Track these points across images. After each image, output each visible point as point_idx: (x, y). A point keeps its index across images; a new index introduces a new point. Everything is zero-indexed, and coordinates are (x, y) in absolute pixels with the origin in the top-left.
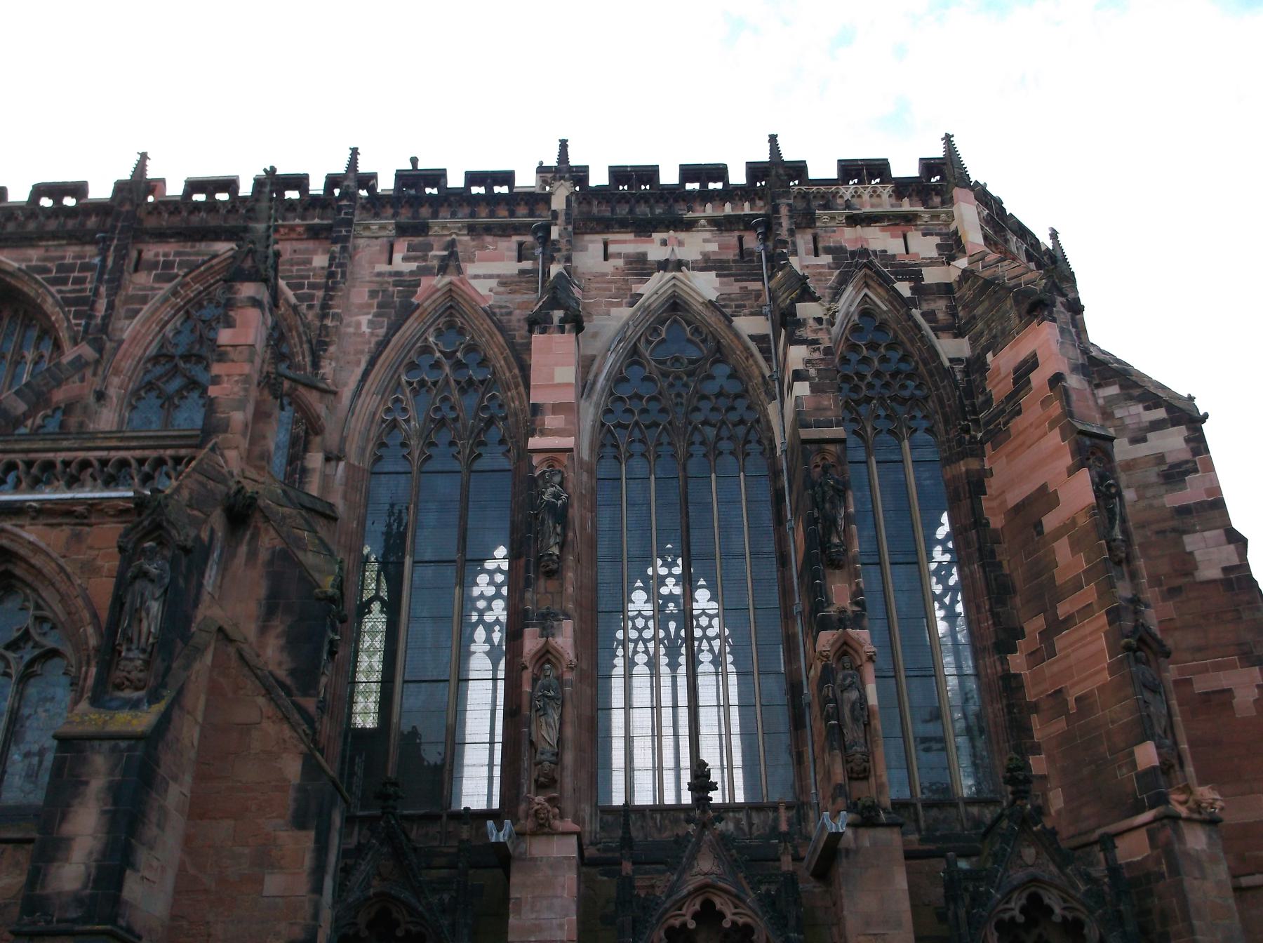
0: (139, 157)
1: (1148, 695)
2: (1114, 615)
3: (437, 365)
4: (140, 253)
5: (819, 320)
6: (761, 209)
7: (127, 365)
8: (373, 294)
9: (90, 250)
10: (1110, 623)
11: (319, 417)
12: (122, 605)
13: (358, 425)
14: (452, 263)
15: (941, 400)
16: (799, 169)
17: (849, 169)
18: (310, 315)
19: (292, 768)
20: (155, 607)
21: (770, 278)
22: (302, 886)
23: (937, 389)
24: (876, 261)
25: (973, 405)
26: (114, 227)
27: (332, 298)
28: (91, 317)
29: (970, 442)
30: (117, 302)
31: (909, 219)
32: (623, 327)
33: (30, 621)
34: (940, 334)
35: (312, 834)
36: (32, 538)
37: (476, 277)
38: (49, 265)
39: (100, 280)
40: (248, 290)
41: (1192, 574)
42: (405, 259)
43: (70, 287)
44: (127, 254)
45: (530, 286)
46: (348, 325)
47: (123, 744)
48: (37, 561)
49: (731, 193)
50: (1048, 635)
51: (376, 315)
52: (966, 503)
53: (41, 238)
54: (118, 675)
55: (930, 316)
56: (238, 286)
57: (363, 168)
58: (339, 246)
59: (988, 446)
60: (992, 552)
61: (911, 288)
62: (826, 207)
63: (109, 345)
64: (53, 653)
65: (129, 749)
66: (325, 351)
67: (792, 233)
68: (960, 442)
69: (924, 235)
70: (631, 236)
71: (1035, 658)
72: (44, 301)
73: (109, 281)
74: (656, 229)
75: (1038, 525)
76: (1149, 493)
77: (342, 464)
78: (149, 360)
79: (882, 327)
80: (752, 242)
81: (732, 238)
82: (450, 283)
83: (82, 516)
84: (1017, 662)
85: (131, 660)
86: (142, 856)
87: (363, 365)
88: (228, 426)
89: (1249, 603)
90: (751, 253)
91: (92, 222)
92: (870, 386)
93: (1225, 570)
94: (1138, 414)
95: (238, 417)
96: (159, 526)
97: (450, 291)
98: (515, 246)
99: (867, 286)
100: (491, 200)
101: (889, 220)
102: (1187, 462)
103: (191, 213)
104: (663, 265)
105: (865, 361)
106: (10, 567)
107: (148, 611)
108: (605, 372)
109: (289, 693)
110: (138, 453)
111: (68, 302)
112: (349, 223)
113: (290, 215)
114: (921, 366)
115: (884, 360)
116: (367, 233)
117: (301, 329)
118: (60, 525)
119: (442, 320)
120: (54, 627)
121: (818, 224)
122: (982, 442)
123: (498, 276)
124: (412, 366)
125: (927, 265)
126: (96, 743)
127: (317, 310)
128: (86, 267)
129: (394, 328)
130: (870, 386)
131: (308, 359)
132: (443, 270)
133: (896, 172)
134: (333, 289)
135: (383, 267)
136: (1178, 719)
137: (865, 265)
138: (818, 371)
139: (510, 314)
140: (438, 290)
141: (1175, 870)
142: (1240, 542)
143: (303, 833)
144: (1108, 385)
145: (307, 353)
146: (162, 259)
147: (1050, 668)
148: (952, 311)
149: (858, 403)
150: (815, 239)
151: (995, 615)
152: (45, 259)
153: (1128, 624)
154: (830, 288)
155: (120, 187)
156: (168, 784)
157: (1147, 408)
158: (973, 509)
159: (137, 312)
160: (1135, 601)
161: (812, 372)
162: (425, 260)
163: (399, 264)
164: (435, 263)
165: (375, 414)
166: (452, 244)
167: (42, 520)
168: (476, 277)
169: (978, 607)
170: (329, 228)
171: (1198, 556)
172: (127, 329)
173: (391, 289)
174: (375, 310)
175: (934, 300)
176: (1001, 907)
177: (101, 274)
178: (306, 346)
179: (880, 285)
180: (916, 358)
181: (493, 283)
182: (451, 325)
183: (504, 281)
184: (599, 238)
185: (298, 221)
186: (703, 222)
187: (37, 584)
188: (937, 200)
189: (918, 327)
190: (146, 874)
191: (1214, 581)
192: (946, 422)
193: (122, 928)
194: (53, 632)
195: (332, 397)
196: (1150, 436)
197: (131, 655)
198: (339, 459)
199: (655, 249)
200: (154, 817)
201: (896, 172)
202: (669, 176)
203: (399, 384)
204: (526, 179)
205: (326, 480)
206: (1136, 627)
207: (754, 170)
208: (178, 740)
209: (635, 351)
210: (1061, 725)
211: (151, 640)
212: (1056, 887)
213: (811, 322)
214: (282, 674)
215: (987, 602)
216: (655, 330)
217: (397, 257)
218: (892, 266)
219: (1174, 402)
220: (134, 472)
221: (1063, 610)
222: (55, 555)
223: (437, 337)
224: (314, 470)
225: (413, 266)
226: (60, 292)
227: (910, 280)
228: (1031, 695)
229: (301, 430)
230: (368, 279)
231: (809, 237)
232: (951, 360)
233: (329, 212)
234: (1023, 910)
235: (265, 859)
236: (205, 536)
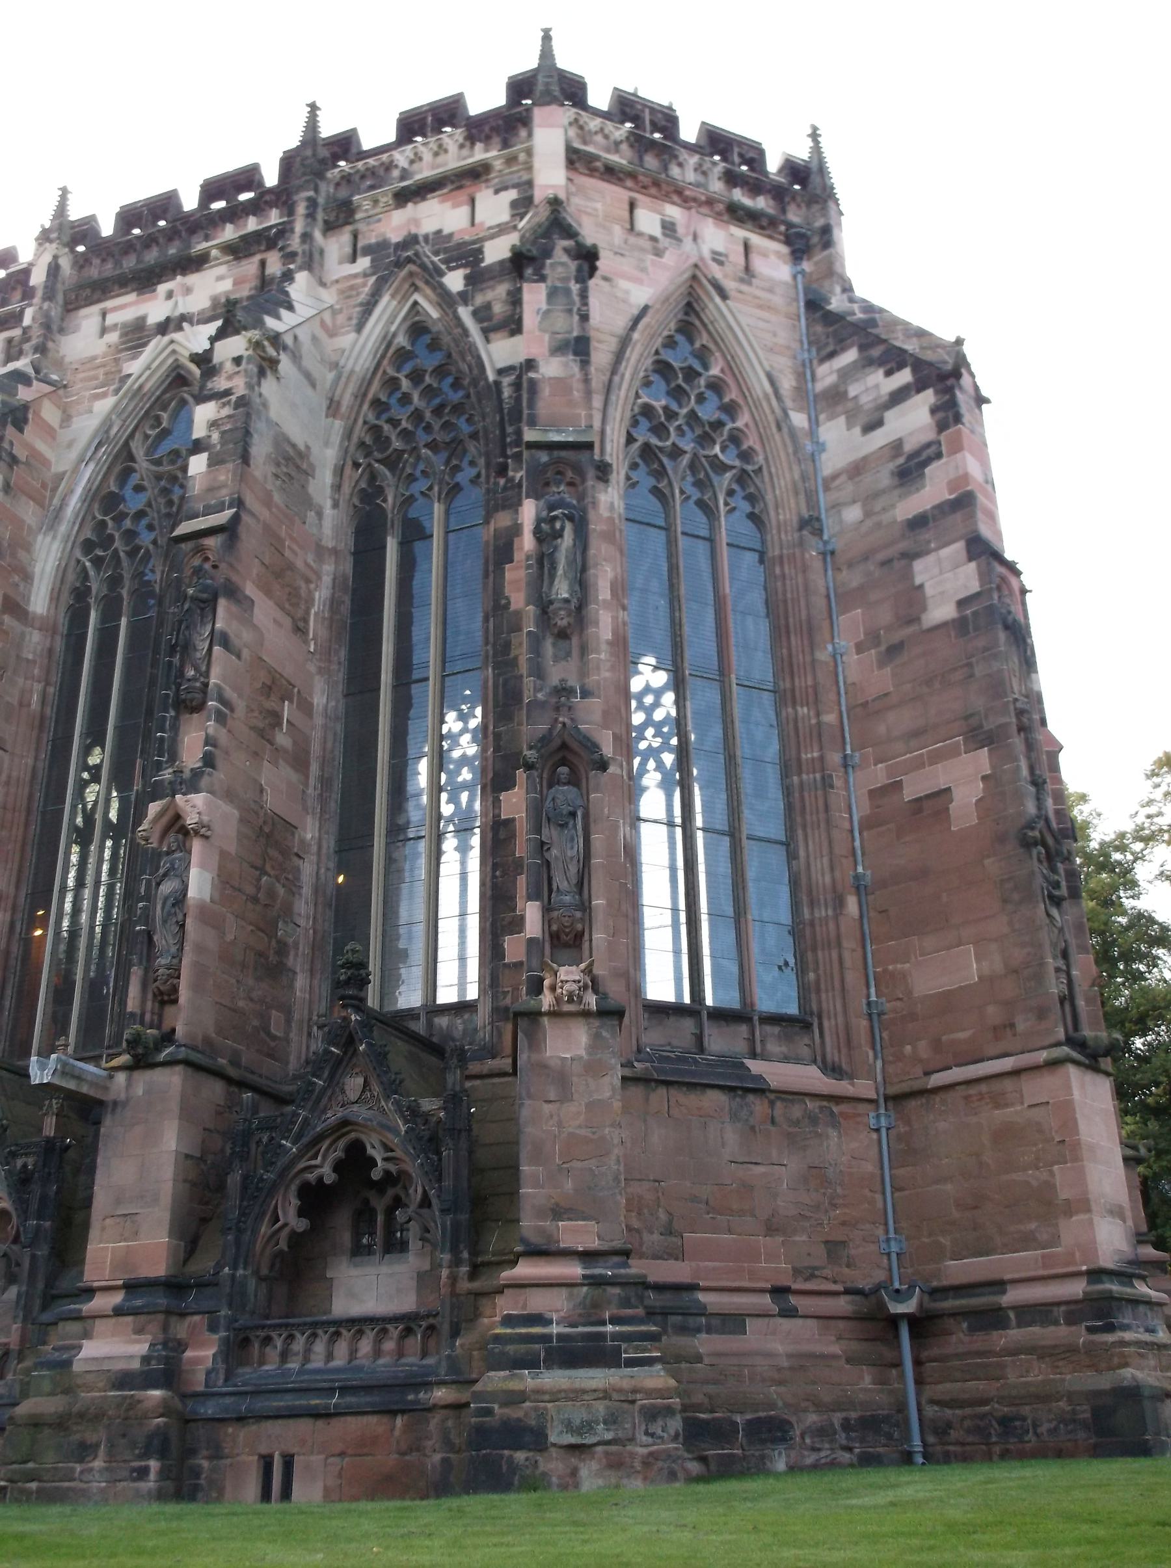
16: (345, 144)
24: (427, 250)
29: (505, 489)
31: (476, 174)
32: (103, 423)
41: (917, 620)
69: (497, 192)
70: (132, 297)
76: (878, 505)
81: (250, 267)
89: (985, 649)
94: (877, 386)
101: (452, 182)
102: (928, 445)
104: (164, 328)
108: (79, 491)
133: (476, 106)
137: (409, 260)
144: (844, 349)
150: (355, 236)
154: (361, 304)
157: (889, 373)
161: (215, 436)
171: (929, 591)
175: (493, 288)
176: (302, 1165)
184: (95, 309)
191: (944, 625)
196: (889, 415)
199: (156, 308)
202: (190, 202)
209: (125, 455)
213: (229, 367)
218: (446, 250)
232: (501, 372)
234: (338, 1167)
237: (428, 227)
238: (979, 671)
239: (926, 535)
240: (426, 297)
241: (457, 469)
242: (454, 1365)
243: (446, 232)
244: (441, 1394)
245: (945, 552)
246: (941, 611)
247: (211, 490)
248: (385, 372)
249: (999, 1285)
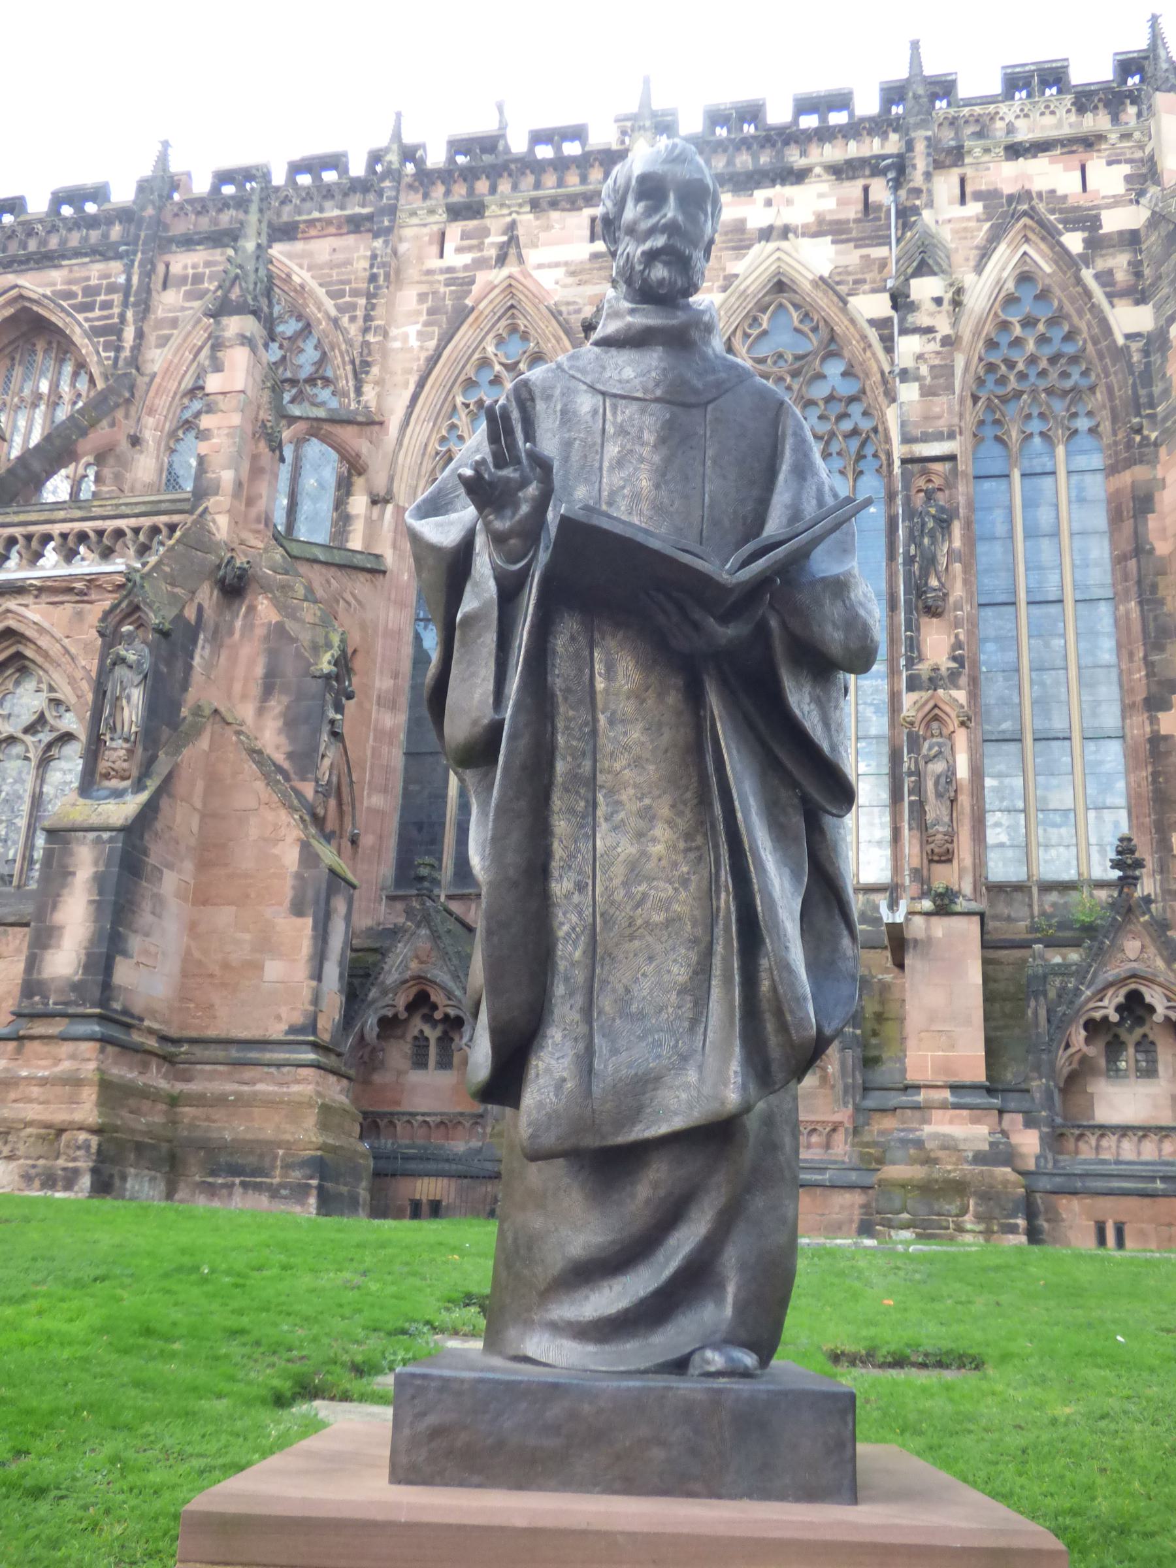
0: (160, 147)
3: (496, 381)
4: (167, 266)
5: (938, 301)
6: (893, 144)
7: (162, 403)
8: (422, 297)
9: (116, 266)
11: (358, 456)
12: (105, 692)
13: (408, 459)
14: (512, 251)
15: (1110, 390)
16: (944, 88)
17: (1015, 82)
18: (353, 330)
19: (290, 857)
20: (137, 694)
21: (898, 241)
22: (300, 971)
23: (1107, 376)
24: (1041, 207)
25: (1150, 396)
26: (138, 236)
27: (373, 307)
28: (118, 349)
29: (1141, 445)
30: (145, 329)
31: (1089, 142)
33: (45, 704)
34: (1116, 301)
35: (309, 922)
36: (36, 617)
37: (540, 266)
38: (74, 288)
39: (125, 304)
40: (234, 325)
42: (459, 250)
43: (97, 313)
44: (154, 269)
45: (604, 273)
46: (395, 339)
47: (106, 835)
48: (43, 642)
49: (855, 130)
51: (427, 324)
52: (1128, 526)
53: (64, 257)
54: (103, 766)
56: (225, 320)
57: (408, 139)
58: (381, 240)
59: (1163, 451)
60: (1154, 587)
62: (980, 135)
63: (142, 381)
64: (67, 737)
65: (111, 840)
66: (367, 373)
67: (928, 176)
68: (1129, 445)
69: (1109, 163)
72: (73, 331)
73: (136, 305)
74: (758, 185)
77: (390, 508)
78: (184, 395)
79: (1043, 296)
80: (881, 192)
81: (854, 189)
82: (510, 277)
83: (82, 593)
85: (115, 749)
86: (135, 943)
87: (412, 387)
88: (218, 487)
90: (879, 207)
91: (116, 232)
92: (1022, 376)
95: (227, 477)
96: (137, 608)
97: (509, 288)
98: (587, 223)
99: (1027, 240)
100: (561, 164)
101: (1063, 146)
103: (220, 210)
104: (766, 234)
105: (1017, 342)
106: (21, 648)
107: (129, 698)
109: (287, 778)
110: (133, 522)
111: (96, 332)
112: (392, 211)
113: (328, 204)
114: (1090, 346)
115: (1043, 340)
116: (415, 220)
117: (343, 347)
118: (62, 603)
119: (503, 323)
120: (68, 710)
121: (967, 160)
122: (1156, 444)
123: (566, 264)
124: (470, 384)
125: (1108, 207)
126: (81, 834)
127: (360, 322)
128: (112, 288)
129: (446, 339)
130: (1022, 376)
131: (351, 383)
132: (501, 260)
133: (1078, 77)
134: (375, 296)
135: (434, 263)
137: (1025, 213)
138: (932, 368)
139: (578, 311)
140: (495, 287)
143: (299, 921)
145: (350, 376)
146: (190, 271)
149: (1004, 400)
150: (963, 181)
151: (1149, 664)
152: (70, 282)
154: (977, 248)
155: (144, 187)
156: (161, 872)
158: (1136, 532)
159: (168, 338)
161: (924, 370)
162: (481, 250)
163: (455, 259)
164: (493, 253)
165: (426, 445)
166: (512, 226)
167: (45, 598)
168: (540, 266)
170: (370, 218)
172: (156, 359)
173: (442, 289)
174: (424, 317)
175: (1113, 255)
176: (1091, 1005)
177: (127, 295)
178: (349, 368)
179: (1043, 239)
180: (1085, 335)
181: (560, 272)
182: (513, 329)
183: (575, 272)
185: (337, 212)
186: (818, 170)
187: (46, 665)
188: (1132, 110)
189: (1088, 294)
190: (143, 960)
192: (1115, 419)
193: (116, 1011)
194: (68, 715)
195: (377, 428)
197: (114, 744)
198: (387, 501)
200: (147, 905)
201: (1078, 77)
203: (455, 407)
204: (603, 136)
205: (372, 526)
207: (893, 94)
208: (170, 828)
211: (134, 729)
212: (1160, 985)
213: (930, 306)
214: (279, 758)
215: (1142, 649)
216: (755, 319)
217: (449, 247)
218: (1061, 211)
220: (130, 544)
222: (59, 635)
223: (498, 345)
224: (358, 516)
225: (467, 258)
226: (87, 320)
227: (1083, 229)
229: (344, 470)
230: (416, 278)
231: (955, 181)
232: (1128, 337)
233: (371, 197)
234: (1119, 1009)
235: (266, 944)
236: (190, 614)
237: (1039, 185)
240: (1039, 251)
241: (1074, 415)
243: (1060, 192)
247: (927, 418)
248: (996, 314)
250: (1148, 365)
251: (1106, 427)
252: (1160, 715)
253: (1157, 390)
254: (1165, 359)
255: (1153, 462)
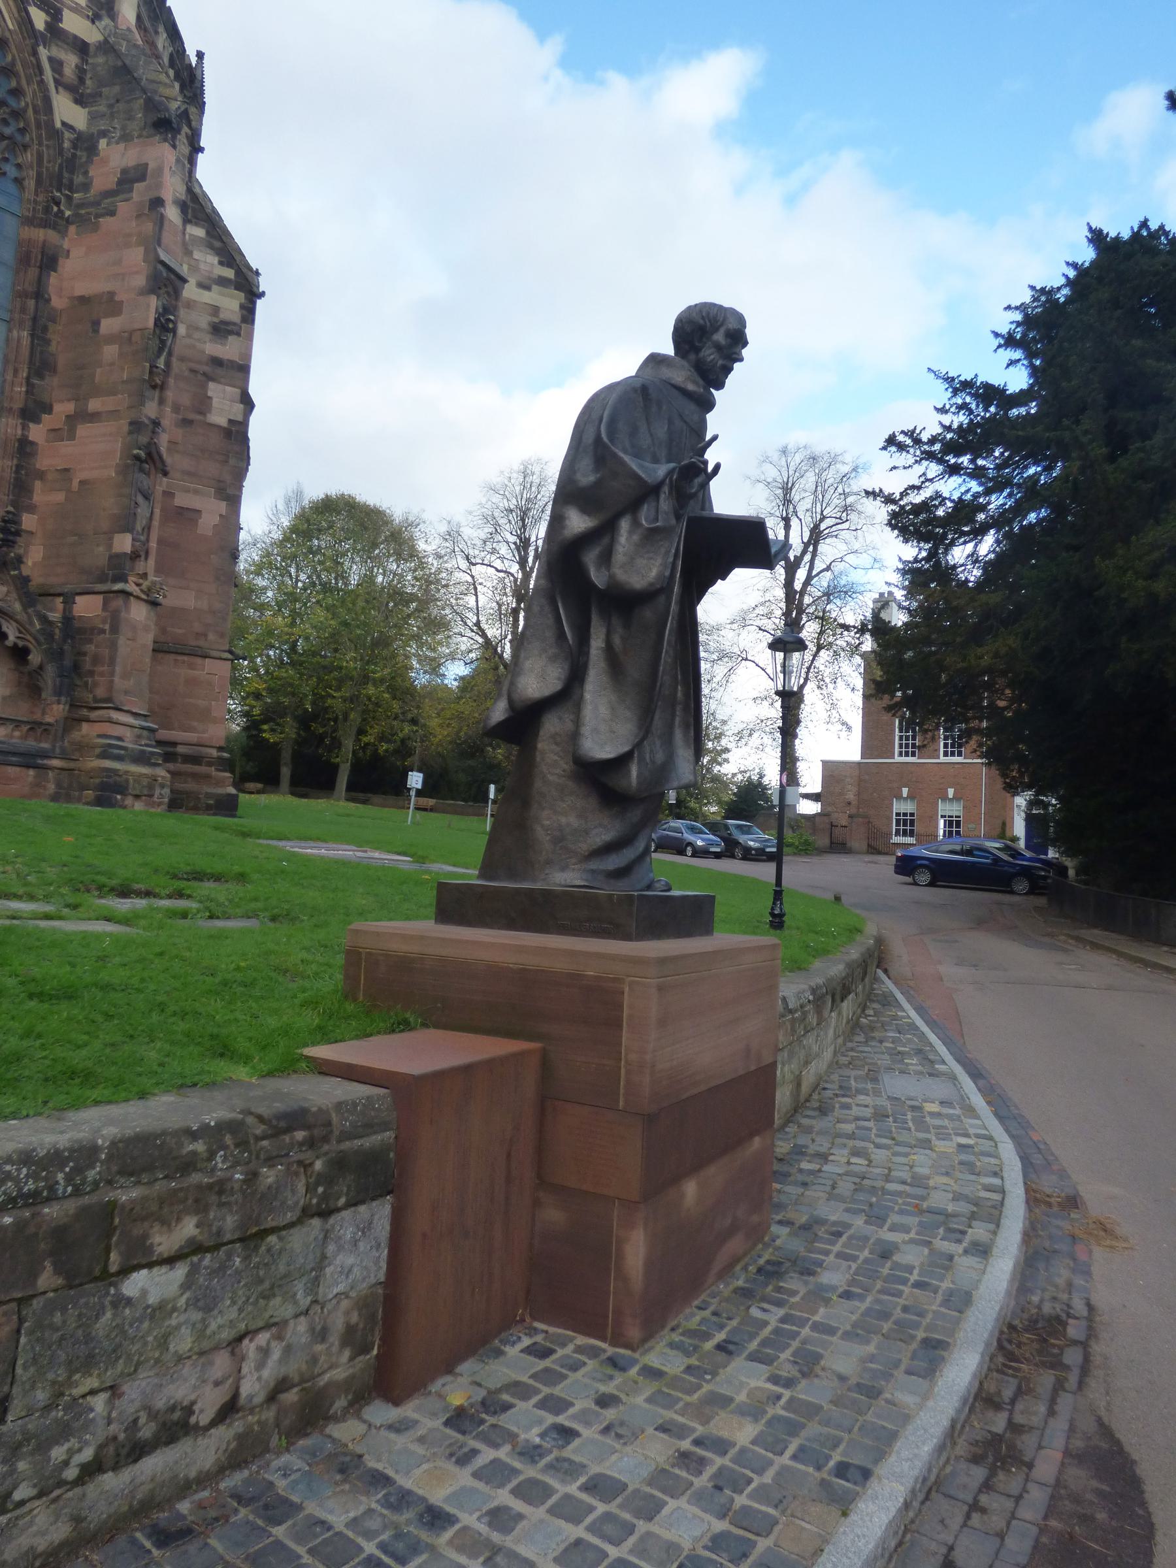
1: (140, 499)
2: (136, 426)
10: (130, 433)
23: (40, 144)
25: (71, 181)
29: (56, 215)
34: (61, 89)
50: (72, 420)
52: (33, 272)
55: (57, 65)
59: (72, 229)
60: (45, 329)
61: (46, 23)
68: (47, 210)
71: (55, 434)
75: (96, 324)
76: (197, 335)
84: (36, 433)
93: (230, 421)
94: (212, 265)
102: (234, 324)
114: (30, 112)
122: (68, 221)
125: (71, 9)
136: (156, 523)
141: (115, 629)
142: (248, 404)
147: (67, 448)
148: (81, 73)
151: (29, 384)
153: (144, 439)
160: (156, 423)
169: (16, 371)
180: (28, 99)
189: (41, 71)
191: (219, 427)
192: (39, 182)
196: (215, 287)
206: (149, 444)
210: (60, 497)
212: (16, 621)
215: (26, 370)
219: (245, 270)
221: (94, 405)
227: (47, 13)
228: (43, 462)
232: (64, 124)
238: (232, 461)
239: (220, 371)
242: (63, 750)
244: (55, 763)
245: (228, 389)
246: (219, 418)
249: (174, 744)
250: (74, 155)
251: (30, 184)
252: (31, 425)
253: (78, 179)
254: (90, 161)
255: (63, 233)
